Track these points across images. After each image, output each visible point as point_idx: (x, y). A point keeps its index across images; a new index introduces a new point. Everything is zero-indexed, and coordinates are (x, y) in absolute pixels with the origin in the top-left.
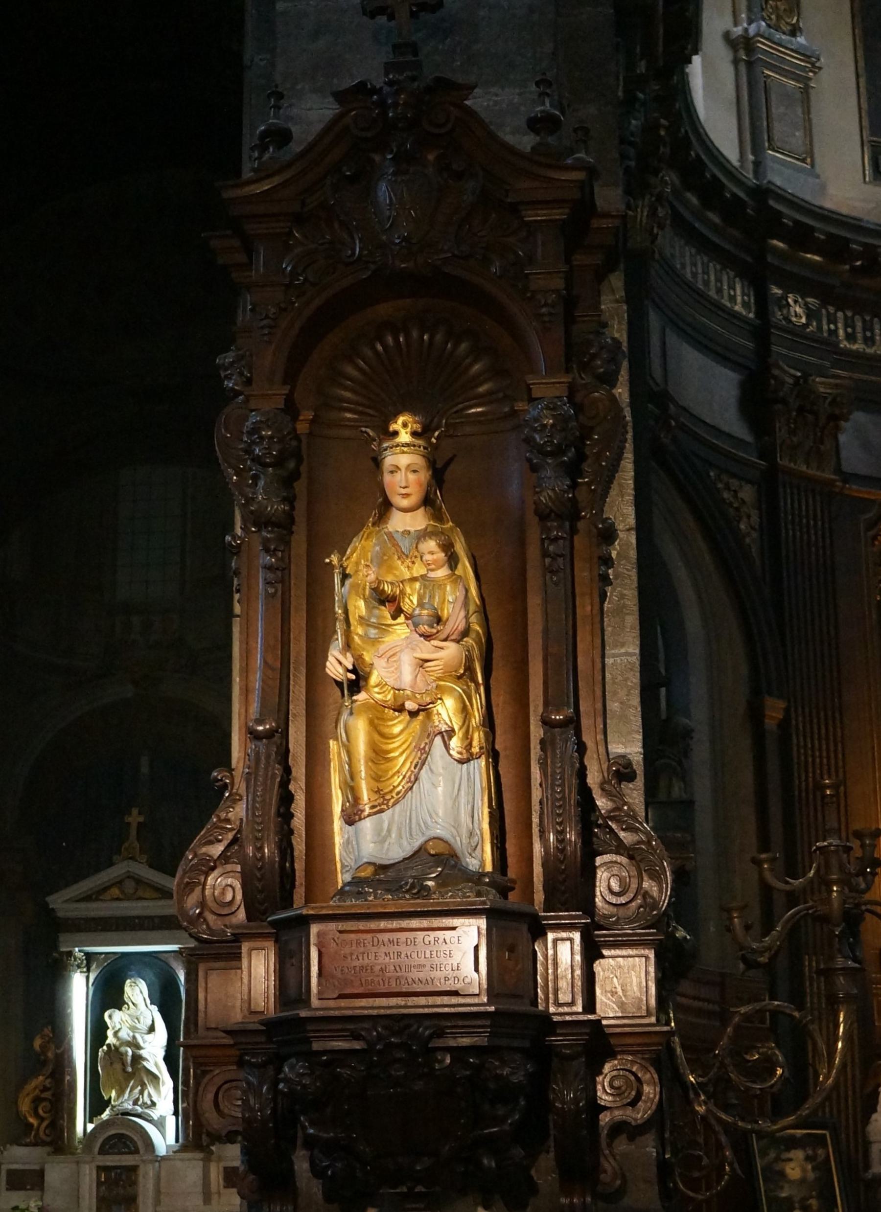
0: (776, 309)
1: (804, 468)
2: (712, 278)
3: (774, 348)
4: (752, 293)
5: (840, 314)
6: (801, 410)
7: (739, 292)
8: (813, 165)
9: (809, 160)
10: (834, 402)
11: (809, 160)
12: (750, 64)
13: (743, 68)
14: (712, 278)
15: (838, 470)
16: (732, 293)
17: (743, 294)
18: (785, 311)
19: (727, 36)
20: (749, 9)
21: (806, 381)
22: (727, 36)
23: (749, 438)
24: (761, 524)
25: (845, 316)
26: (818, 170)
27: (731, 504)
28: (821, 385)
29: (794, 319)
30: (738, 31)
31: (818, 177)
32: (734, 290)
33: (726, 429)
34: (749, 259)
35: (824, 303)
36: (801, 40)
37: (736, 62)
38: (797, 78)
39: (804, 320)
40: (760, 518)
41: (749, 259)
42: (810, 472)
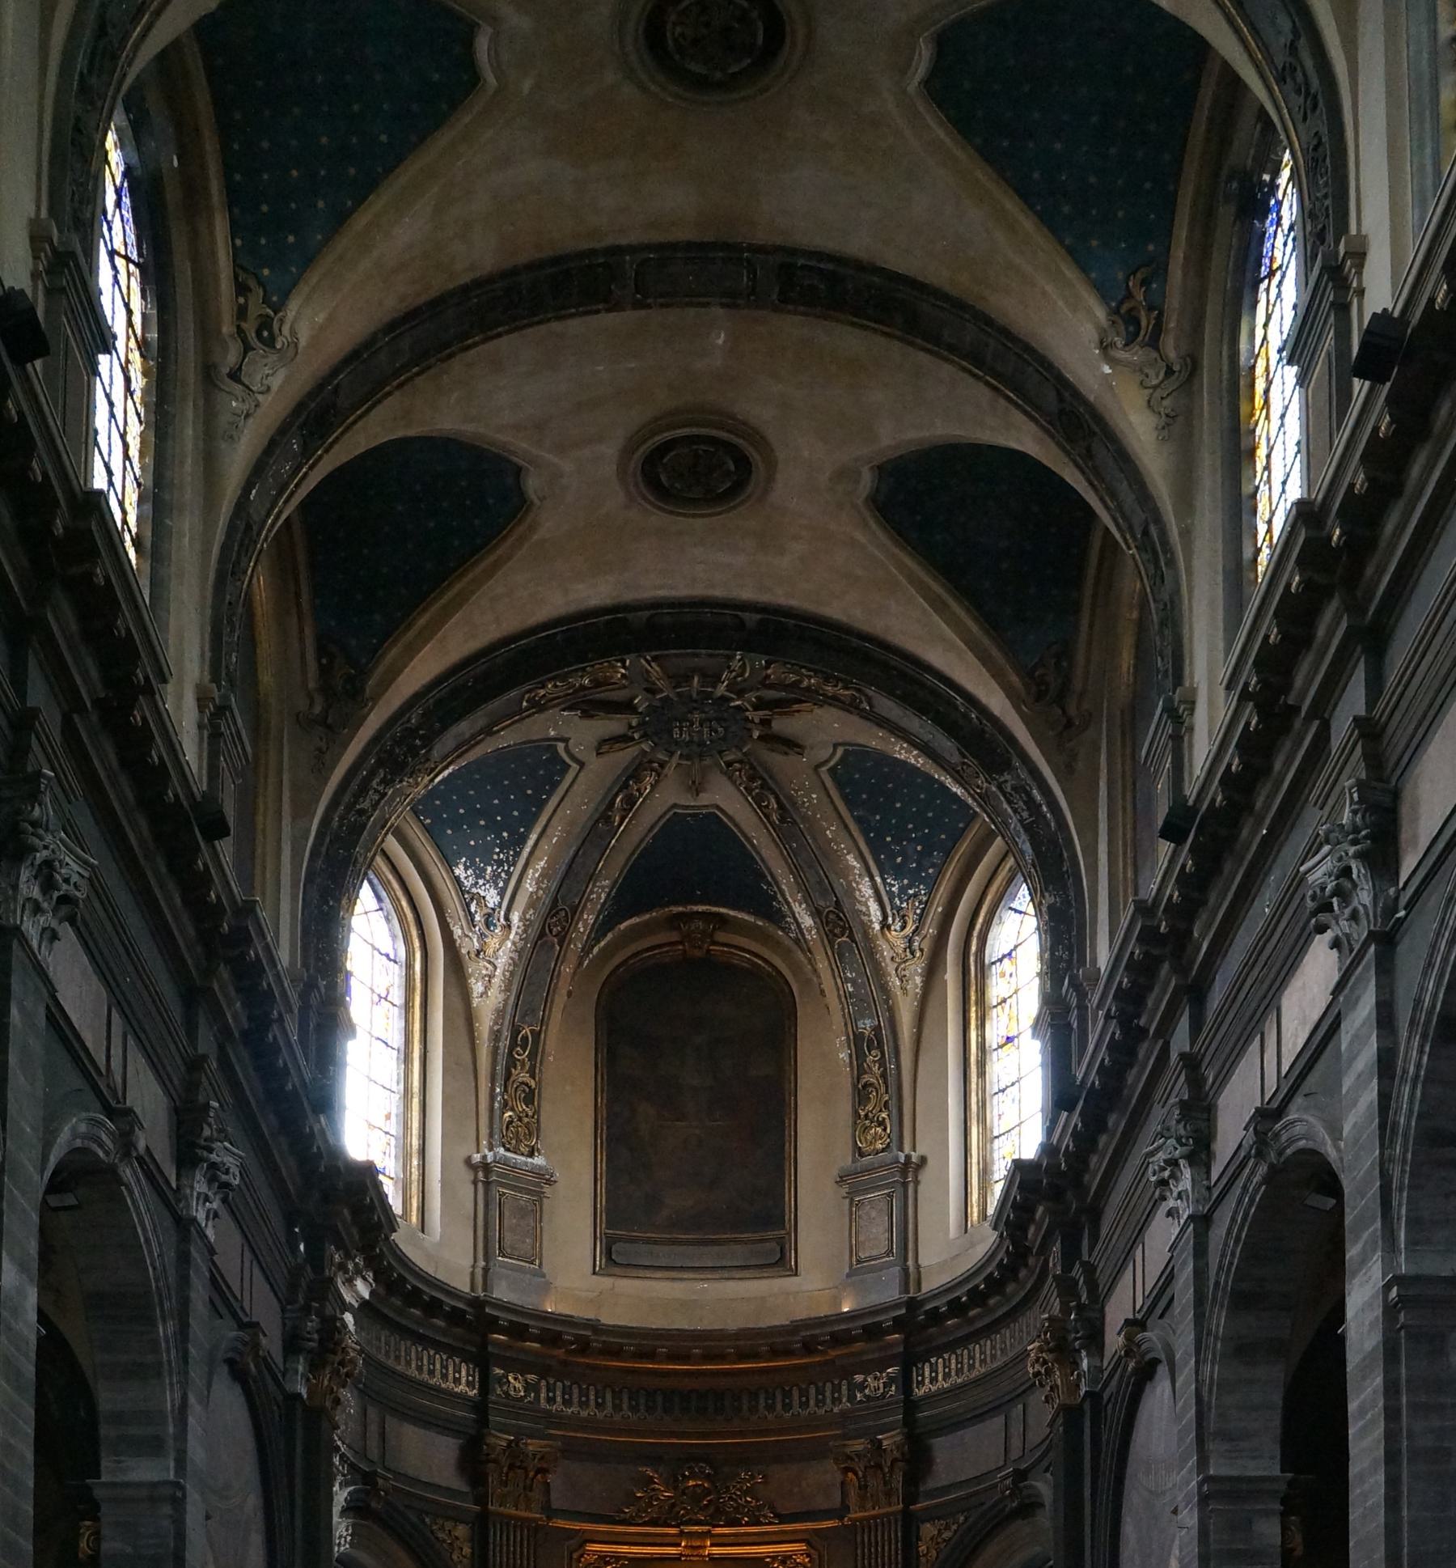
0: (497, 1386)
1: (513, 1511)
2: (438, 1366)
3: (491, 1418)
4: (477, 1374)
5: (559, 1384)
6: (511, 1467)
7: (464, 1373)
8: (540, 1265)
9: (537, 1262)
10: (542, 1458)
11: (537, 1262)
12: (487, 1184)
13: (480, 1185)
14: (438, 1366)
15: (550, 1512)
16: (457, 1375)
17: (468, 1375)
18: (505, 1388)
19: (468, 1161)
20: (491, 1135)
21: (517, 1445)
22: (468, 1161)
23: (465, 1489)
24: (473, 1553)
25: (564, 1385)
26: (545, 1270)
27: (444, 1541)
28: (533, 1446)
29: (512, 1393)
30: (477, 1158)
31: (544, 1276)
32: (460, 1373)
33: (444, 1484)
34: (474, 1350)
35: (542, 1376)
36: (538, 1161)
37: (475, 1183)
38: (529, 1191)
39: (522, 1394)
40: (472, 1548)
41: (474, 1350)
42: (518, 1513)
